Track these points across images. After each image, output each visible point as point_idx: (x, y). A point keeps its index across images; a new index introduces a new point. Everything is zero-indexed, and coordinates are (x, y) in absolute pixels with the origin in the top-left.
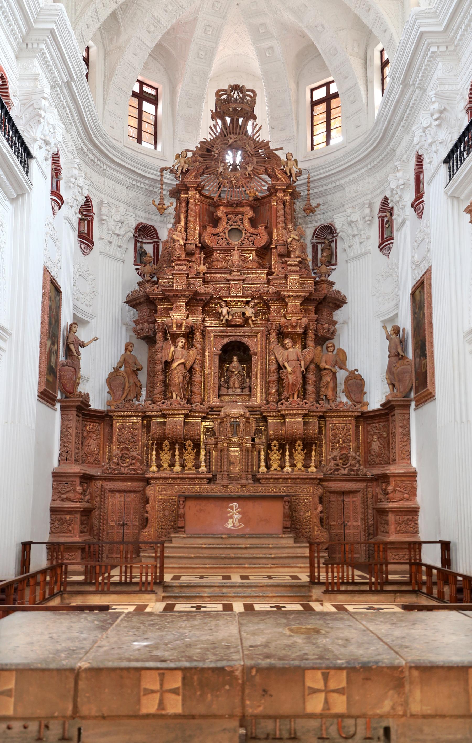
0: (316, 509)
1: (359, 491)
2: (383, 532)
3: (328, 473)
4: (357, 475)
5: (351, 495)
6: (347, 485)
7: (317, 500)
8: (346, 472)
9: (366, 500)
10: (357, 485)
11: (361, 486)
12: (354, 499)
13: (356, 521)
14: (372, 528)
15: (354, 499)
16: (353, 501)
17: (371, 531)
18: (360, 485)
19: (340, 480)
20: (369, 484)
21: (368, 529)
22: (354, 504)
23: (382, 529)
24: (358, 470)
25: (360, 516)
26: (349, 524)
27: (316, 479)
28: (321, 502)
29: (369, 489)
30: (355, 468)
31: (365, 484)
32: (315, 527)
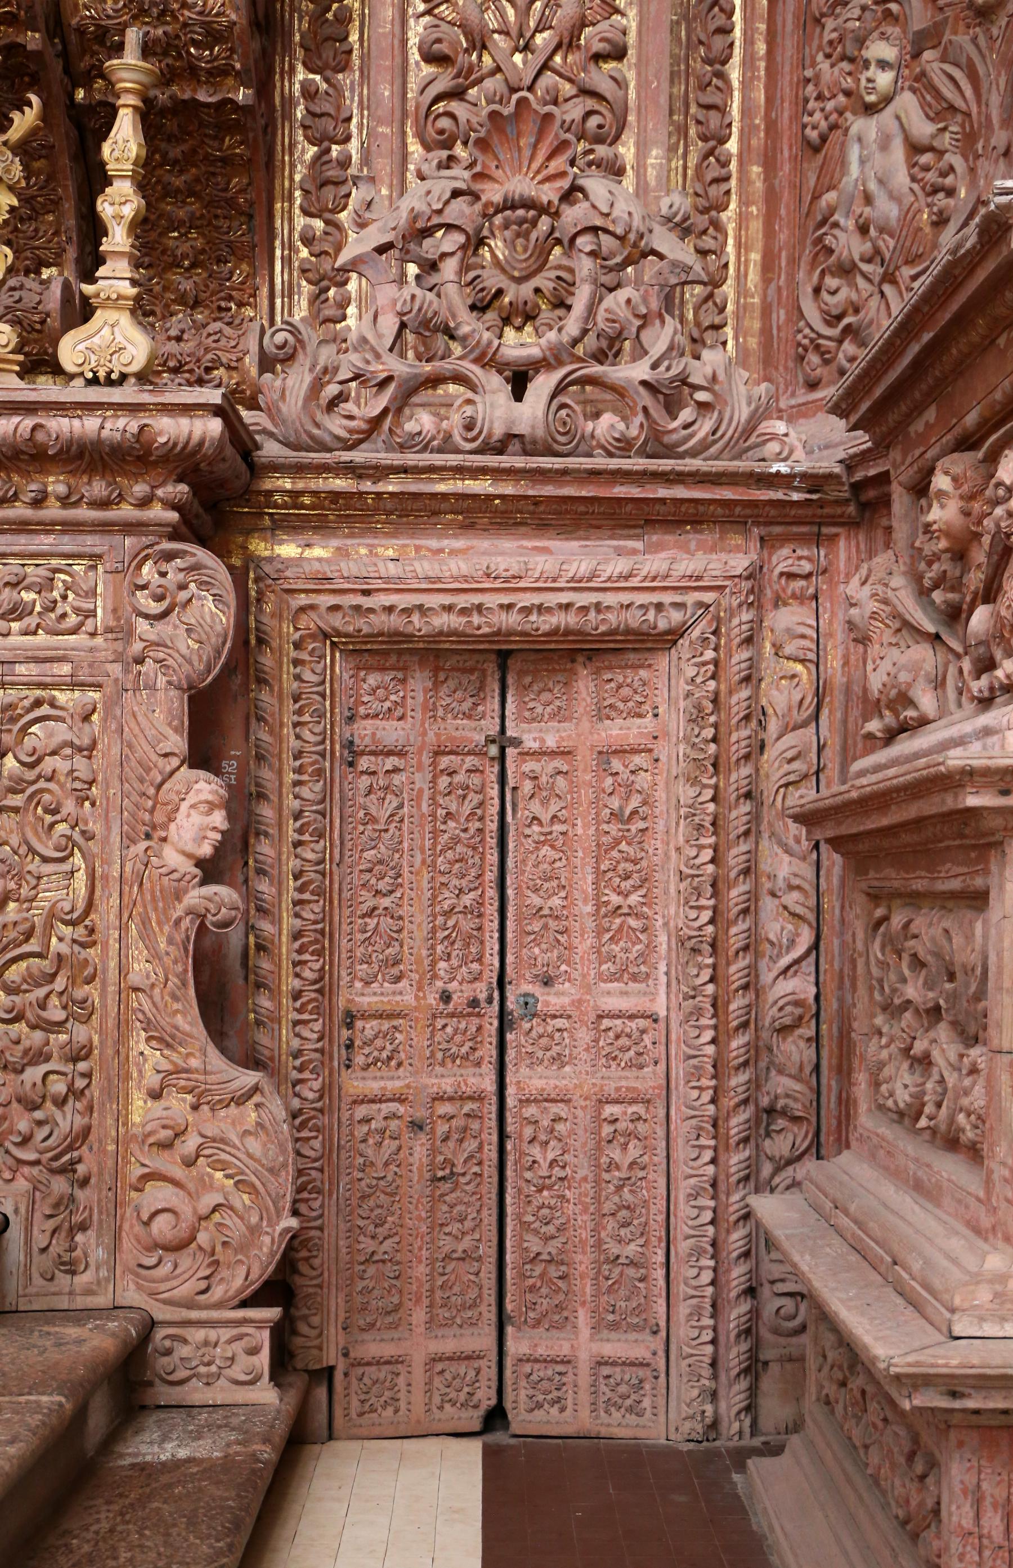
0: (153, 832)
1: (671, 638)
2: (908, 1116)
3: (336, 425)
4: (657, 445)
5: (585, 685)
6: (542, 564)
7: (160, 723)
8: (530, 413)
9: (739, 737)
10: (655, 563)
11: (695, 582)
12: (617, 730)
13: (626, 974)
14: (795, 1050)
15: (617, 730)
16: (605, 755)
17: (781, 1085)
18: (687, 565)
19: (475, 515)
20: (784, 559)
21: (756, 1055)
22: (621, 771)
23: (902, 1085)
24: (671, 394)
25: (673, 914)
26: (551, 1000)
27: (133, 458)
28: (202, 755)
29: (788, 618)
30: (639, 371)
31: (740, 563)
32: (138, 1042)
